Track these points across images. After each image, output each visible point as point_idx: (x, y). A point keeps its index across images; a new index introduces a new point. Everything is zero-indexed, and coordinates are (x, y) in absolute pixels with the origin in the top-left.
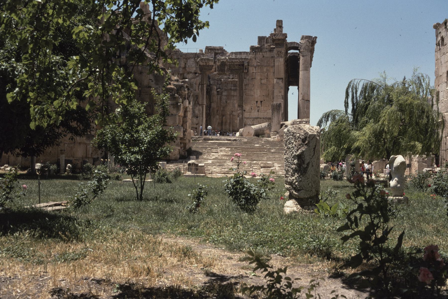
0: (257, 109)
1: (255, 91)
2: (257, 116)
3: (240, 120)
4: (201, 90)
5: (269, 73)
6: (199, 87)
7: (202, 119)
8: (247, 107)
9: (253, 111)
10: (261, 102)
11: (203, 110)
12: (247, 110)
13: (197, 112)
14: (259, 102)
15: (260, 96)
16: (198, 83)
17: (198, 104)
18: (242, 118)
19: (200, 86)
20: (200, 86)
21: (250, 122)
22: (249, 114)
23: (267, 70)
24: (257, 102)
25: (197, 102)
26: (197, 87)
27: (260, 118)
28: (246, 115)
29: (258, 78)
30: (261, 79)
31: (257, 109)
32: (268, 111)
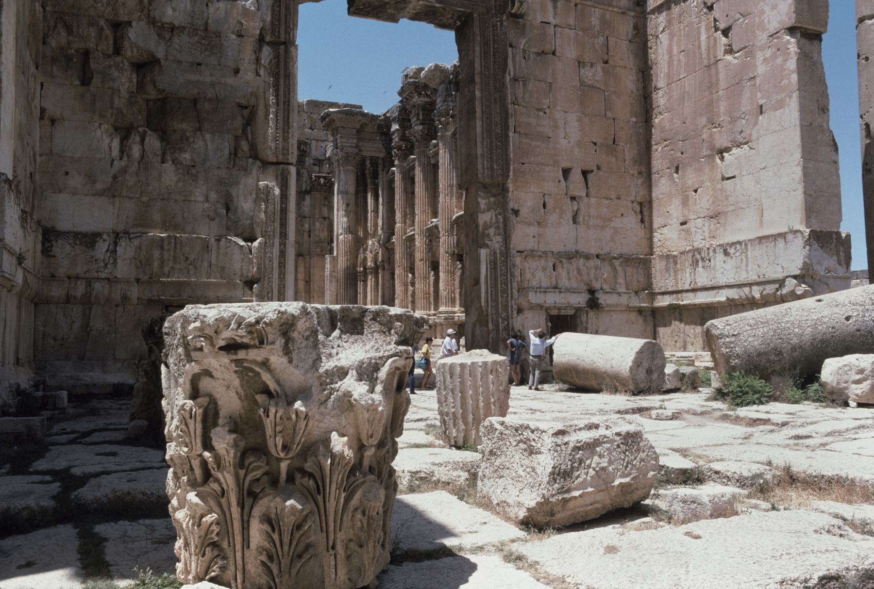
0: (570, 208)
1: (559, 115)
2: (571, 247)
3: (493, 264)
4: (276, 76)
5: (612, 41)
6: (258, 51)
7: (283, 254)
8: (524, 197)
9: (553, 218)
10: (585, 173)
11: (284, 196)
12: (523, 212)
13: (245, 205)
14: (576, 176)
15: (579, 144)
16: (254, 27)
17: (255, 155)
18: (506, 253)
19: (266, 51)
20: (266, 51)
21: (540, 274)
22: (533, 230)
23: (603, 21)
24: (566, 172)
25: (245, 146)
26: (248, 55)
27: (587, 257)
28: (523, 236)
29: (570, 53)
30: (580, 63)
31: (570, 208)
32: (617, 223)
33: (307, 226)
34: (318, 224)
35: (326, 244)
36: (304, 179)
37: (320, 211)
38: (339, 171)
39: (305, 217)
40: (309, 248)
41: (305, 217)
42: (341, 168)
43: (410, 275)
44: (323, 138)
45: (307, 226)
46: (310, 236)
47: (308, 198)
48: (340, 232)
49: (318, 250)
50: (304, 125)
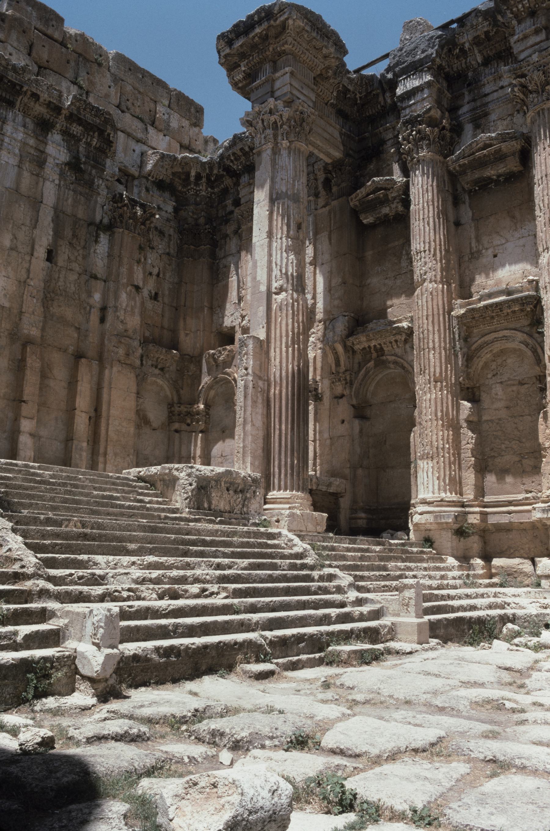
33: (97, 297)
34: (124, 296)
35: (136, 343)
36: (100, 200)
37: (131, 272)
38: (276, 151)
39: (95, 277)
40: (102, 344)
41: (95, 277)
42: (285, 143)
43: (466, 404)
44: (140, 135)
45: (97, 297)
46: (102, 320)
47: (104, 239)
48: (275, 285)
49: (121, 351)
50: (107, 96)
